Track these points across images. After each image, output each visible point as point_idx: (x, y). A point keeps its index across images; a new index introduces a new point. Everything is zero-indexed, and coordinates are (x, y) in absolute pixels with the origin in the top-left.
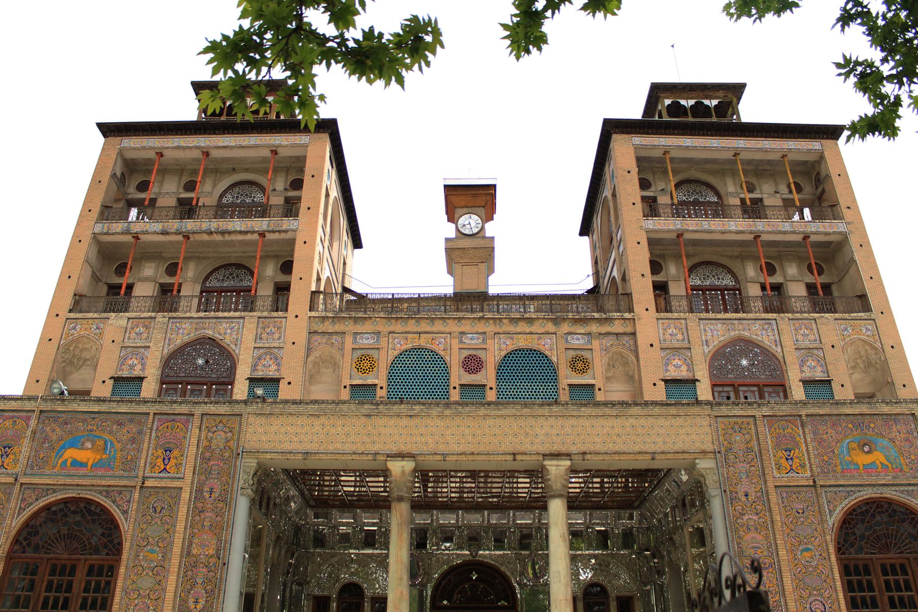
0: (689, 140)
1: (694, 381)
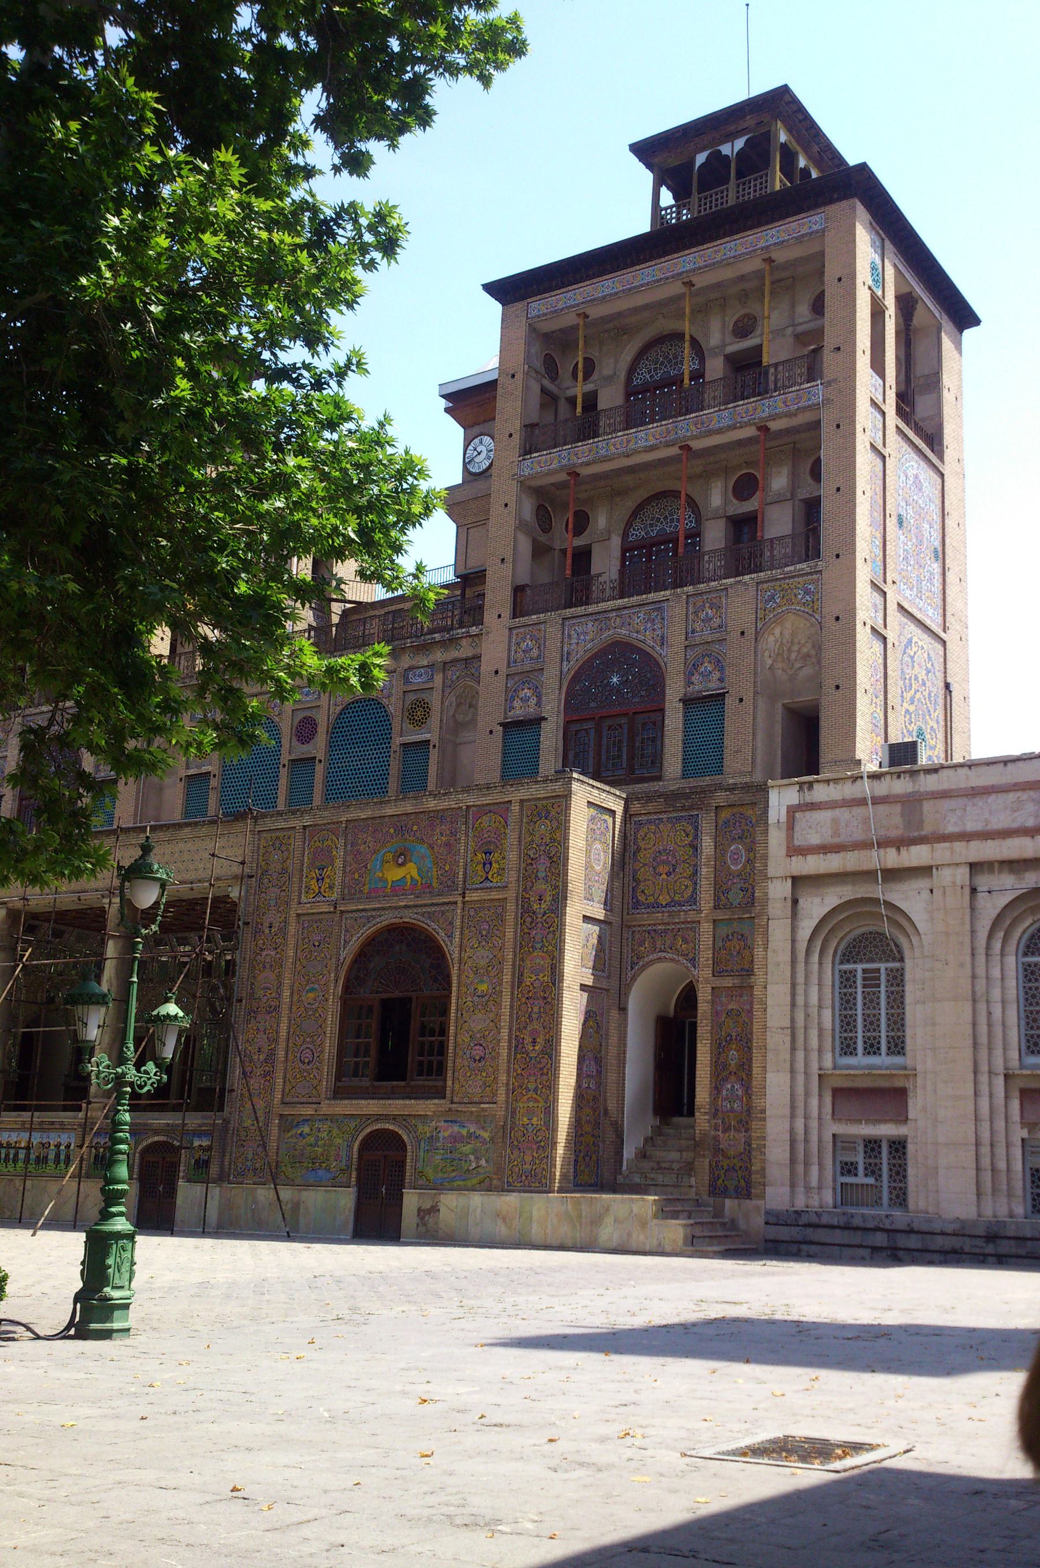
0: (610, 283)
1: (537, 721)
